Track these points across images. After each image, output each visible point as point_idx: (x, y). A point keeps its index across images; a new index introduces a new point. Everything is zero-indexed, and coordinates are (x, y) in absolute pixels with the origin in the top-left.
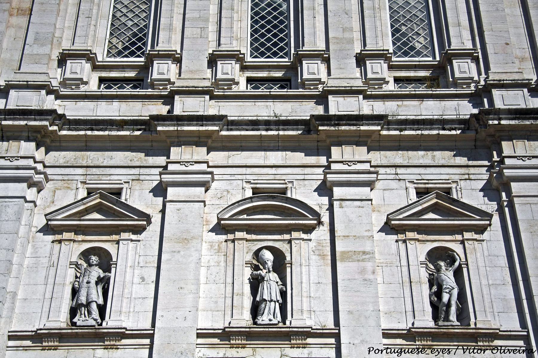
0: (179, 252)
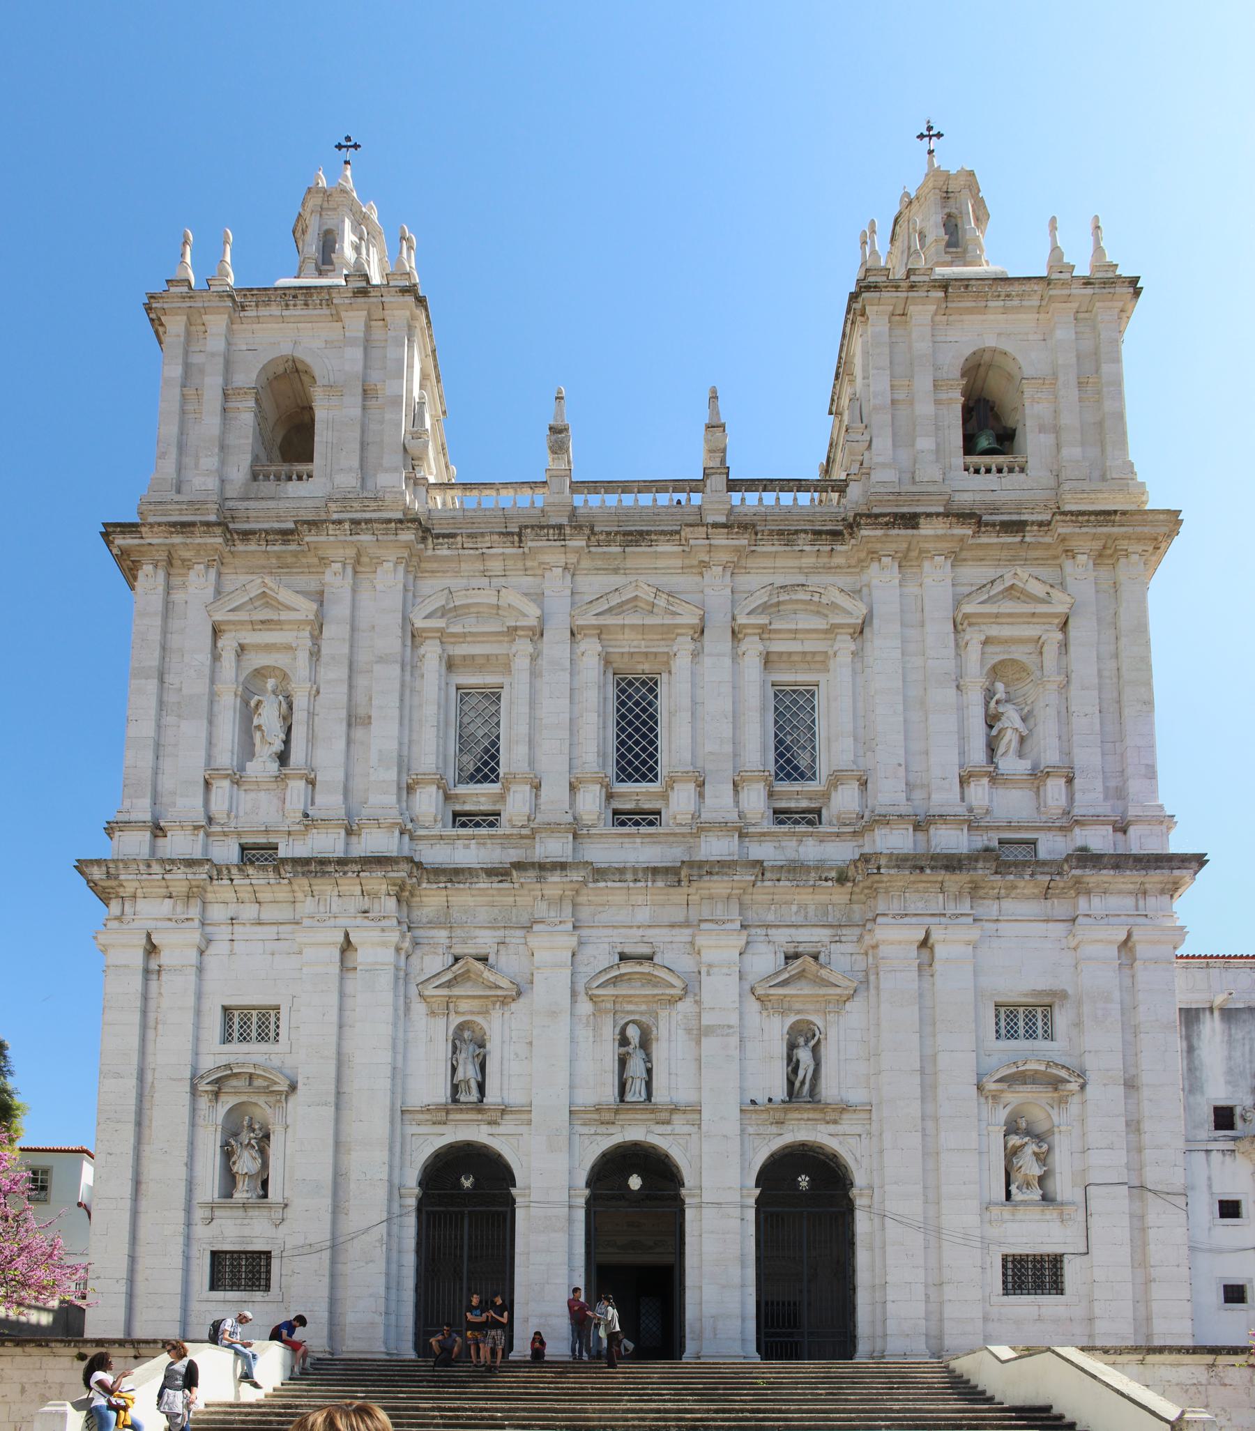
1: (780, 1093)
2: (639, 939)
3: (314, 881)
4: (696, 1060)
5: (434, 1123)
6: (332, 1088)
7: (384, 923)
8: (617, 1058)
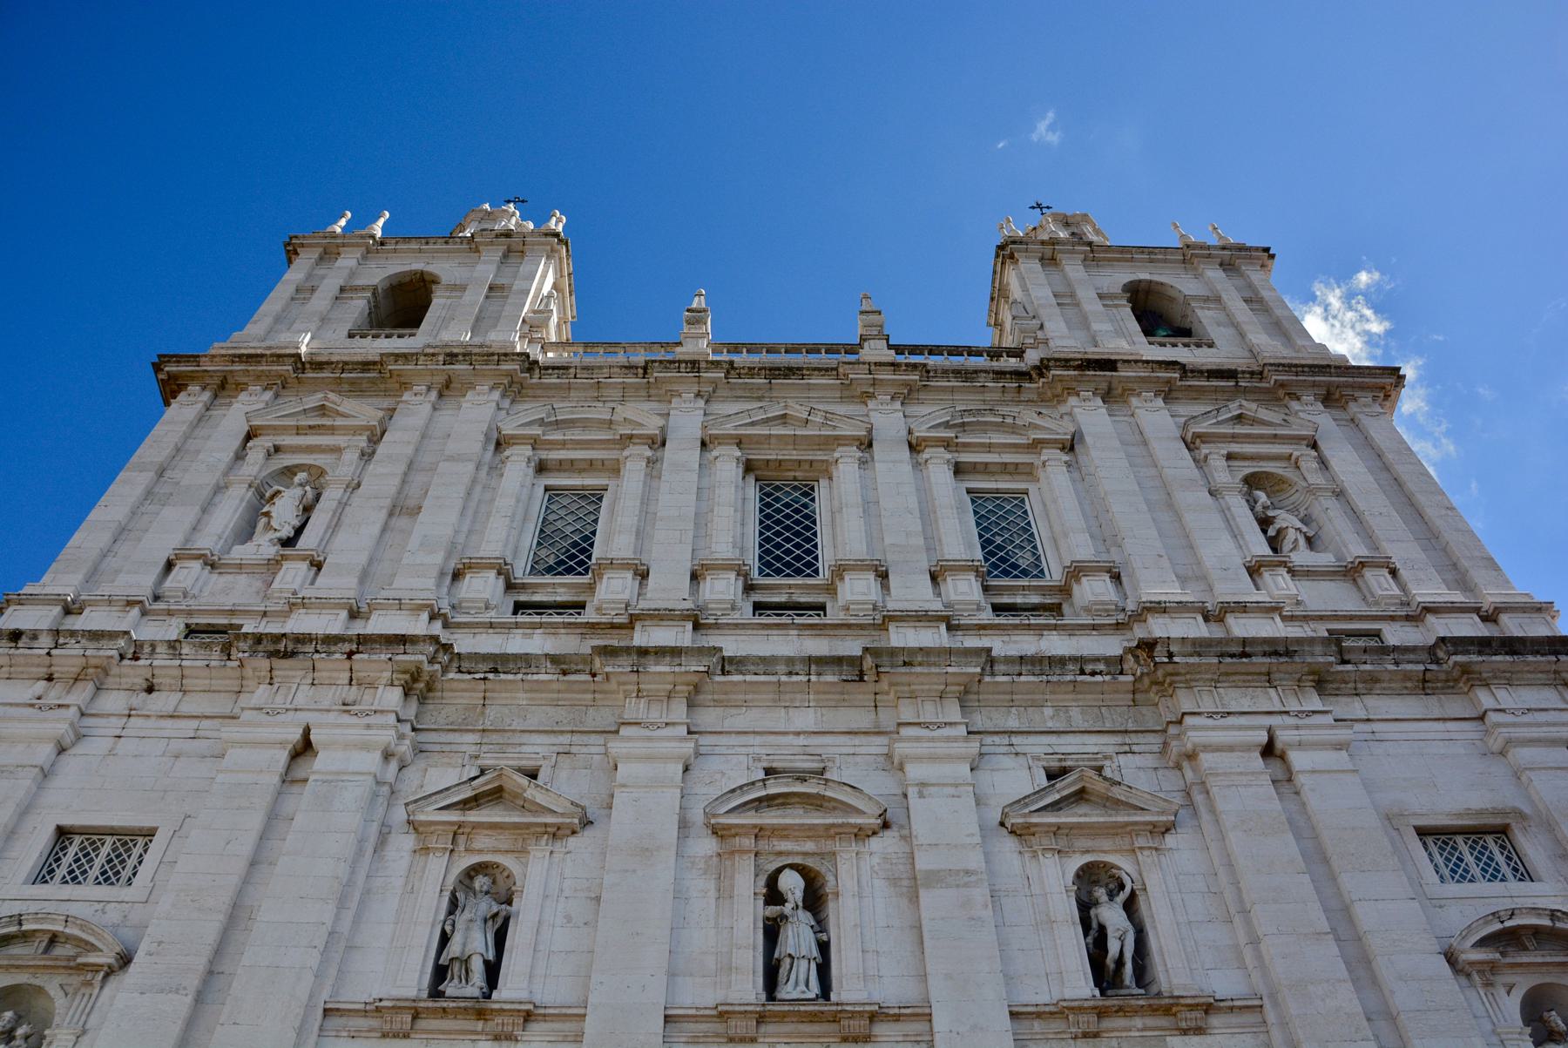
0: (634, 871)
1: (1081, 986)
2: (800, 750)
4: (912, 927)
5: (384, 1036)
6: (200, 963)
7: (372, 720)
8: (761, 925)
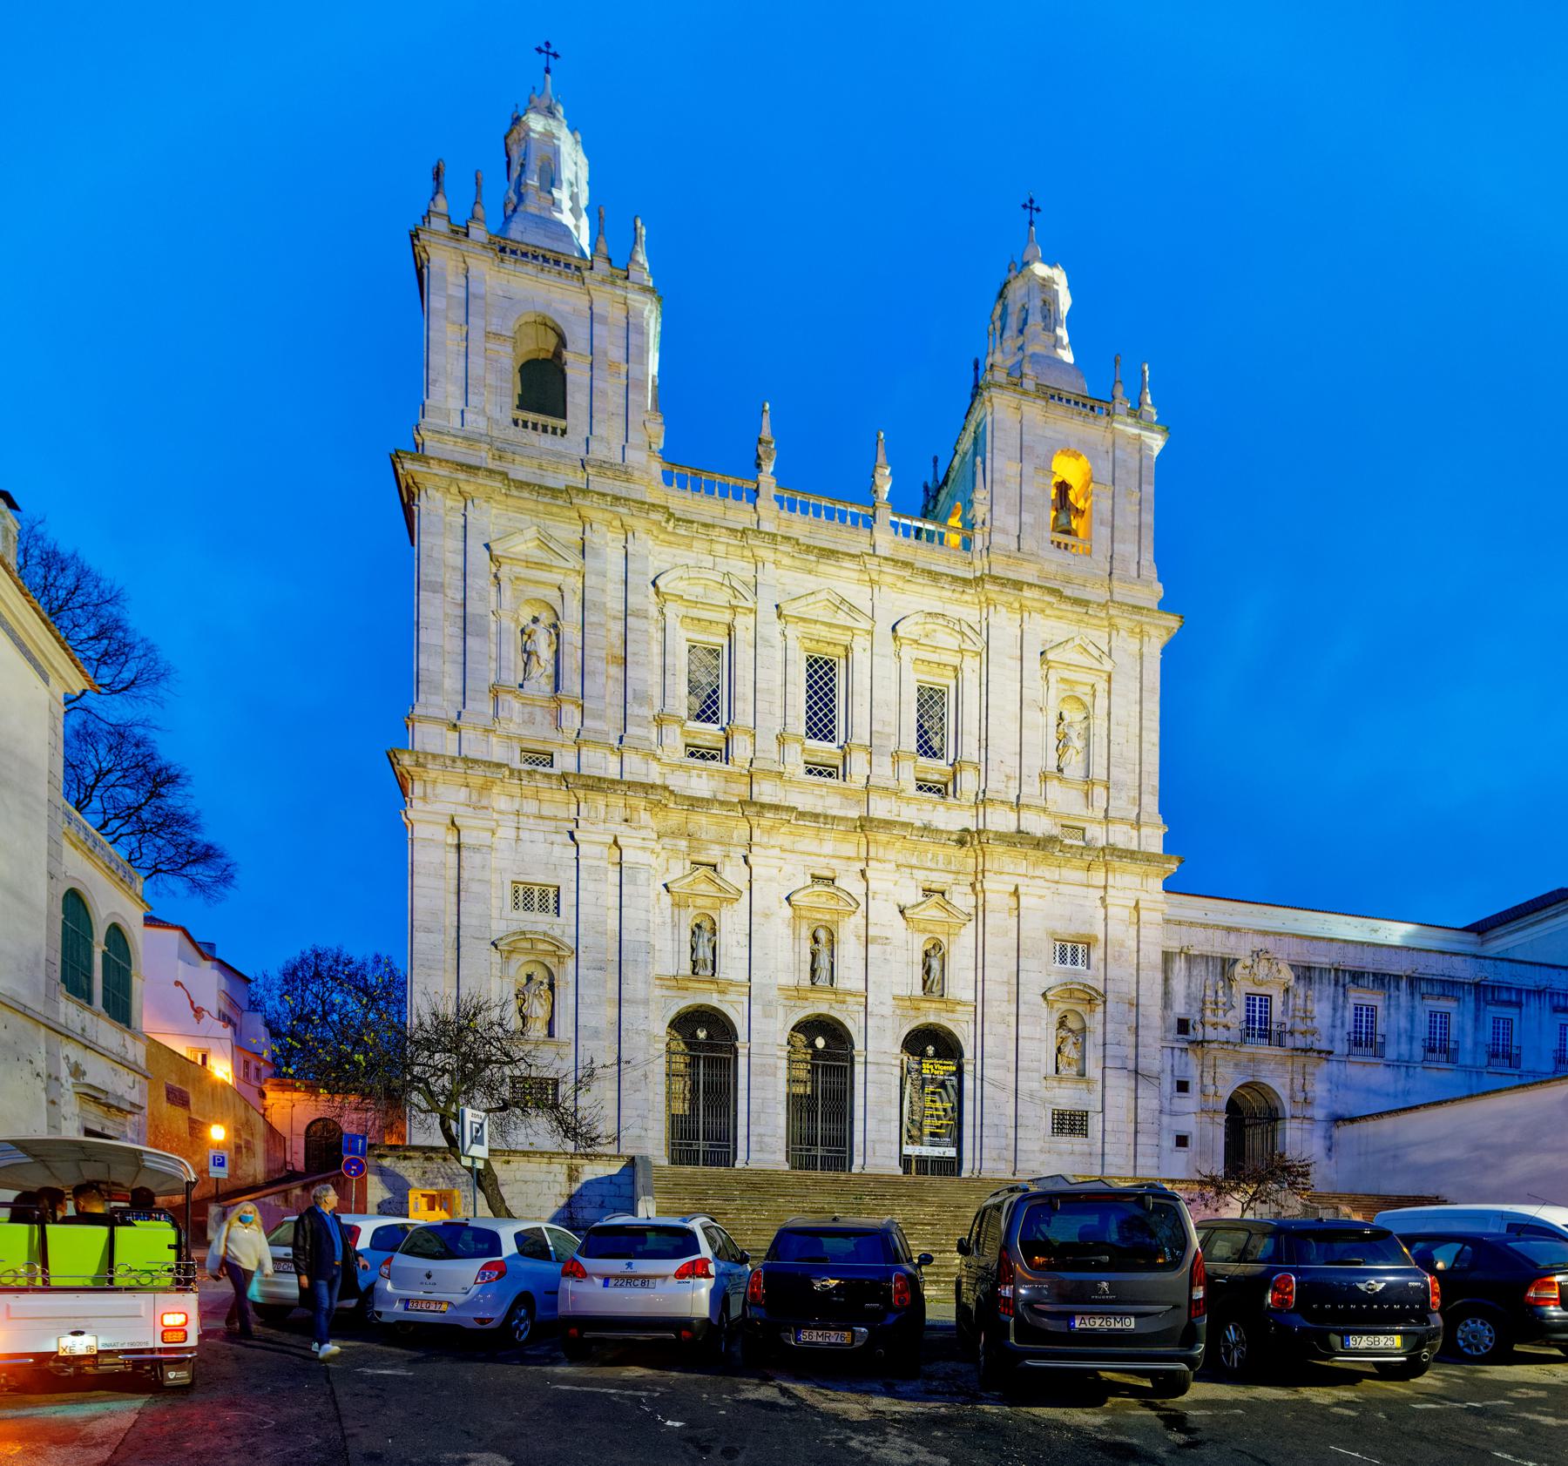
3: (588, 792)
